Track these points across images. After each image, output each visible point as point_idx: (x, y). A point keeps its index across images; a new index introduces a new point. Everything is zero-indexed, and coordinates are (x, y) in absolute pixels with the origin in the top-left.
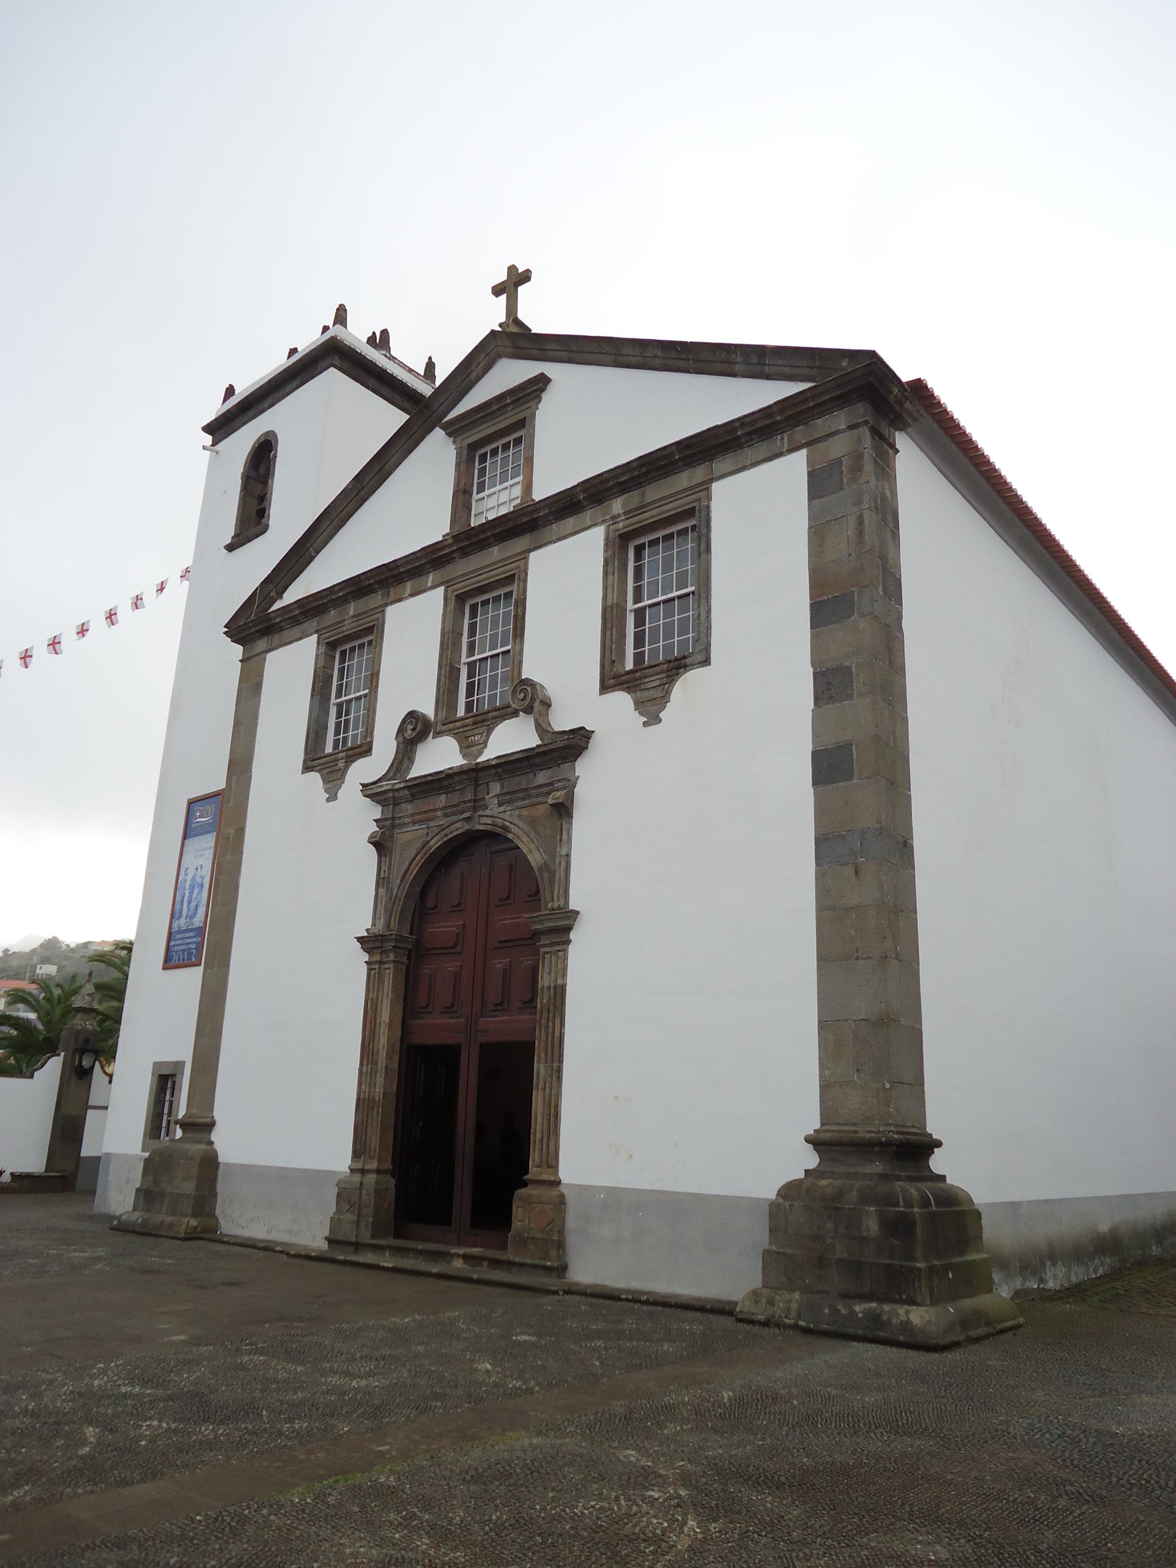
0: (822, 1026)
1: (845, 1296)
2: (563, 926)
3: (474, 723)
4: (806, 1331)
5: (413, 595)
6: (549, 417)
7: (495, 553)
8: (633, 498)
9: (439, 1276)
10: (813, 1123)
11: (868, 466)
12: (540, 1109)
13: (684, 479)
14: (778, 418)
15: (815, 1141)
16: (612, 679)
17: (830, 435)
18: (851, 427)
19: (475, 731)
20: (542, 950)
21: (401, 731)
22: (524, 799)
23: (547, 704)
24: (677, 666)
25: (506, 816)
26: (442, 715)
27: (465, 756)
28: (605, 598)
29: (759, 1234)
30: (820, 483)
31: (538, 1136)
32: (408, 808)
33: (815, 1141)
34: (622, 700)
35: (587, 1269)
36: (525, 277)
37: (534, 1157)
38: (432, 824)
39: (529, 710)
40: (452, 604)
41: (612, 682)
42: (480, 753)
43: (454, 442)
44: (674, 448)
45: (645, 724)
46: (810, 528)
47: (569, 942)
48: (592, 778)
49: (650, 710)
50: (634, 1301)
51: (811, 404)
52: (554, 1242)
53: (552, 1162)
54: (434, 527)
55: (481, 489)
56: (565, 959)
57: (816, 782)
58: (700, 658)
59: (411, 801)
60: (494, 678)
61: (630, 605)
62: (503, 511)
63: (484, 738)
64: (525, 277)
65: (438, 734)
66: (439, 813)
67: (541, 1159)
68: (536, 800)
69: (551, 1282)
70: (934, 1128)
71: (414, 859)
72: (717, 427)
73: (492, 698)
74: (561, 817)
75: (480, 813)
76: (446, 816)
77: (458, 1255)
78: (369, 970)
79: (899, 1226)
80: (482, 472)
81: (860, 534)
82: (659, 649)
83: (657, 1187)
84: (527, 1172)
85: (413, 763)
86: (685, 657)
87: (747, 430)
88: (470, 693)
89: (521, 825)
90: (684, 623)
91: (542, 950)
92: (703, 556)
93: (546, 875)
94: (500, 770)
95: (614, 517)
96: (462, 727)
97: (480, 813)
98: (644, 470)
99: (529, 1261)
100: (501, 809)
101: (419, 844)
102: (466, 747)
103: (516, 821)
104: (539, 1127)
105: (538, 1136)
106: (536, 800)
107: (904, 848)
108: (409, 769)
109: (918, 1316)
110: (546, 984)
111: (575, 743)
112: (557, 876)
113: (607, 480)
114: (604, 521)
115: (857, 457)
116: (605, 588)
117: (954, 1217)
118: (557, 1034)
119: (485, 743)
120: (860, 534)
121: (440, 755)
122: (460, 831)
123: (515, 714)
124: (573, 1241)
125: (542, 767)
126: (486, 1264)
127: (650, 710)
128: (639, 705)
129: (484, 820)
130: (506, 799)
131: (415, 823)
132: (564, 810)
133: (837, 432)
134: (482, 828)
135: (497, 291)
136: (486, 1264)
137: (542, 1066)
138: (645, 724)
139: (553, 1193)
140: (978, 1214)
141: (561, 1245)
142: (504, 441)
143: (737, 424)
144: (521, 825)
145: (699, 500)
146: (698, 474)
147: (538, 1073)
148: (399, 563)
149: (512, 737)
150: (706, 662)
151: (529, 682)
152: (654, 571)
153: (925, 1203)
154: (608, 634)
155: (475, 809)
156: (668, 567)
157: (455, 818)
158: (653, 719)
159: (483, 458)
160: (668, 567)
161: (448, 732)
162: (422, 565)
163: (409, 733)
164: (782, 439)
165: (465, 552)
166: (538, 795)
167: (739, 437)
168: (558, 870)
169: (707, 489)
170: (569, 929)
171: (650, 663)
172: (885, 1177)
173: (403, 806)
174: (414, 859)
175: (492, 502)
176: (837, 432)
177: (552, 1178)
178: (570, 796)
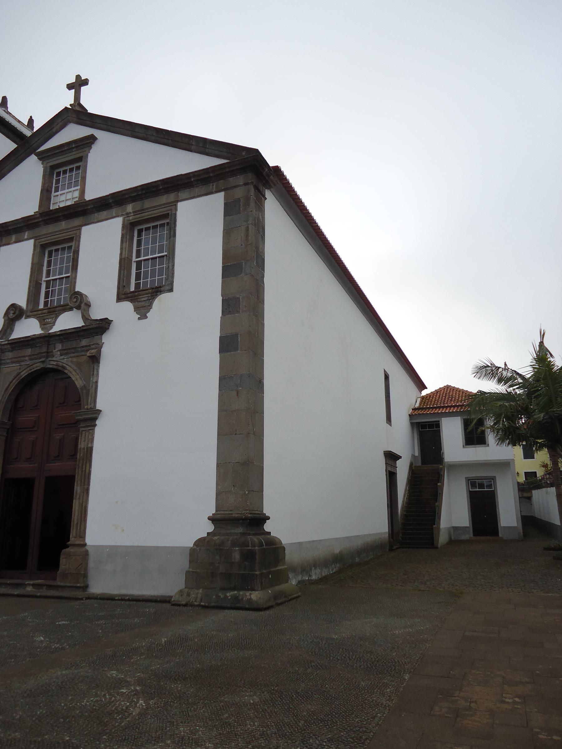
0: (218, 465)
1: (223, 589)
2: (93, 416)
3: (49, 312)
4: (204, 607)
5: (16, 242)
6: (95, 158)
7: (63, 225)
8: (138, 205)
9: (18, 596)
10: (212, 510)
11: (252, 204)
12: (77, 509)
13: (164, 199)
14: (211, 175)
15: (212, 519)
16: (123, 295)
17: (235, 187)
18: (245, 184)
19: (49, 317)
20: (81, 429)
21: (7, 314)
22: (74, 353)
23: (88, 305)
24: (156, 291)
25: (65, 361)
26: (30, 307)
27: (42, 329)
28: (121, 254)
29: (184, 563)
30: (230, 209)
31: (75, 522)
32: (10, 355)
33: (212, 519)
34: (128, 306)
35: (98, 586)
36: (85, 82)
37: (73, 533)
38: (23, 363)
39: (78, 308)
40: (38, 250)
41: (123, 296)
42: (51, 328)
43: (42, 164)
44: (159, 183)
45: (139, 319)
46: (224, 230)
47: (95, 425)
48: (110, 344)
49: (142, 311)
50: (122, 600)
51: (227, 170)
52: (82, 574)
53: (82, 535)
54: (29, 207)
55: (57, 190)
56: (93, 434)
57: (221, 351)
58: (168, 288)
59: (12, 351)
60: (60, 290)
61: (134, 259)
62: (69, 203)
63: (53, 320)
64: (85, 82)
65: (28, 317)
66: (27, 358)
67: (76, 534)
68: (81, 354)
69: (79, 594)
70: (267, 511)
71: (11, 382)
72: (181, 175)
73: (59, 300)
74: (93, 363)
75: (50, 359)
76: (31, 360)
77: (29, 585)
79: (248, 556)
80: (58, 182)
81: (247, 236)
82: (148, 282)
83: (136, 544)
84: (69, 541)
85: (12, 330)
86: (160, 287)
87: (196, 178)
88: (47, 296)
89: (72, 366)
90: (161, 270)
91: (81, 429)
92: (172, 238)
93: (85, 392)
94: (61, 337)
95: (127, 214)
96: (41, 314)
97: (50, 359)
98: (144, 192)
99: (69, 585)
100: (62, 357)
101: (15, 374)
102: (43, 325)
103: (70, 364)
104: (76, 518)
105: (75, 522)
106: (81, 354)
107: (260, 384)
108: (10, 334)
109: (255, 596)
110: (82, 446)
111: (104, 325)
112: (90, 392)
114: (122, 215)
115: (247, 199)
116: (121, 249)
117: (274, 550)
118: (87, 471)
119: (54, 324)
120: (247, 236)
121: (29, 328)
122: (38, 368)
123: (71, 309)
124: (92, 573)
125: (85, 337)
126: (45, 587)
127: (142, 311)
128: (136, 309)
130: (64, 352)
131: (13, 363)
132: (95, 359)
133: (239, 186)
134: (51, 366)
135: (70, 87)
136: (45, 587)
137: (79, 488)
138: (139, 319)
139: (82, 550)
140: (284, 548)
141: (85, 576)
142: (71, 166)
143: (191, 175)
144: (72, 366)
145: (171, 210)
146: (171, 197)
147: (77, 491)
149: (69, 321)
150: (171, 290)
151: (79, 293)
152: (147, 243)
153: (261, 545)
154: (122, 272)
155: (47, 357)
156: (154, 242)
157: (35, 361)
158: (143, 316)
159: (58, 174)
160: (154, 242)
161: (34, 316)
162: (22, 227)
163: (11, 315)
164: (213, 185)
165: (47, 222)
166: (82, 351)
167: (192, 182)
168: (91, 389)
169: (175, 205)
170: (96, 419)
171: (143, 288)
172: (243, 534)
173: (7, 354)
174: (11, 382)
175: (63, 198)
176: (239, 186)
177: (82, 543)
178: (99, 352)
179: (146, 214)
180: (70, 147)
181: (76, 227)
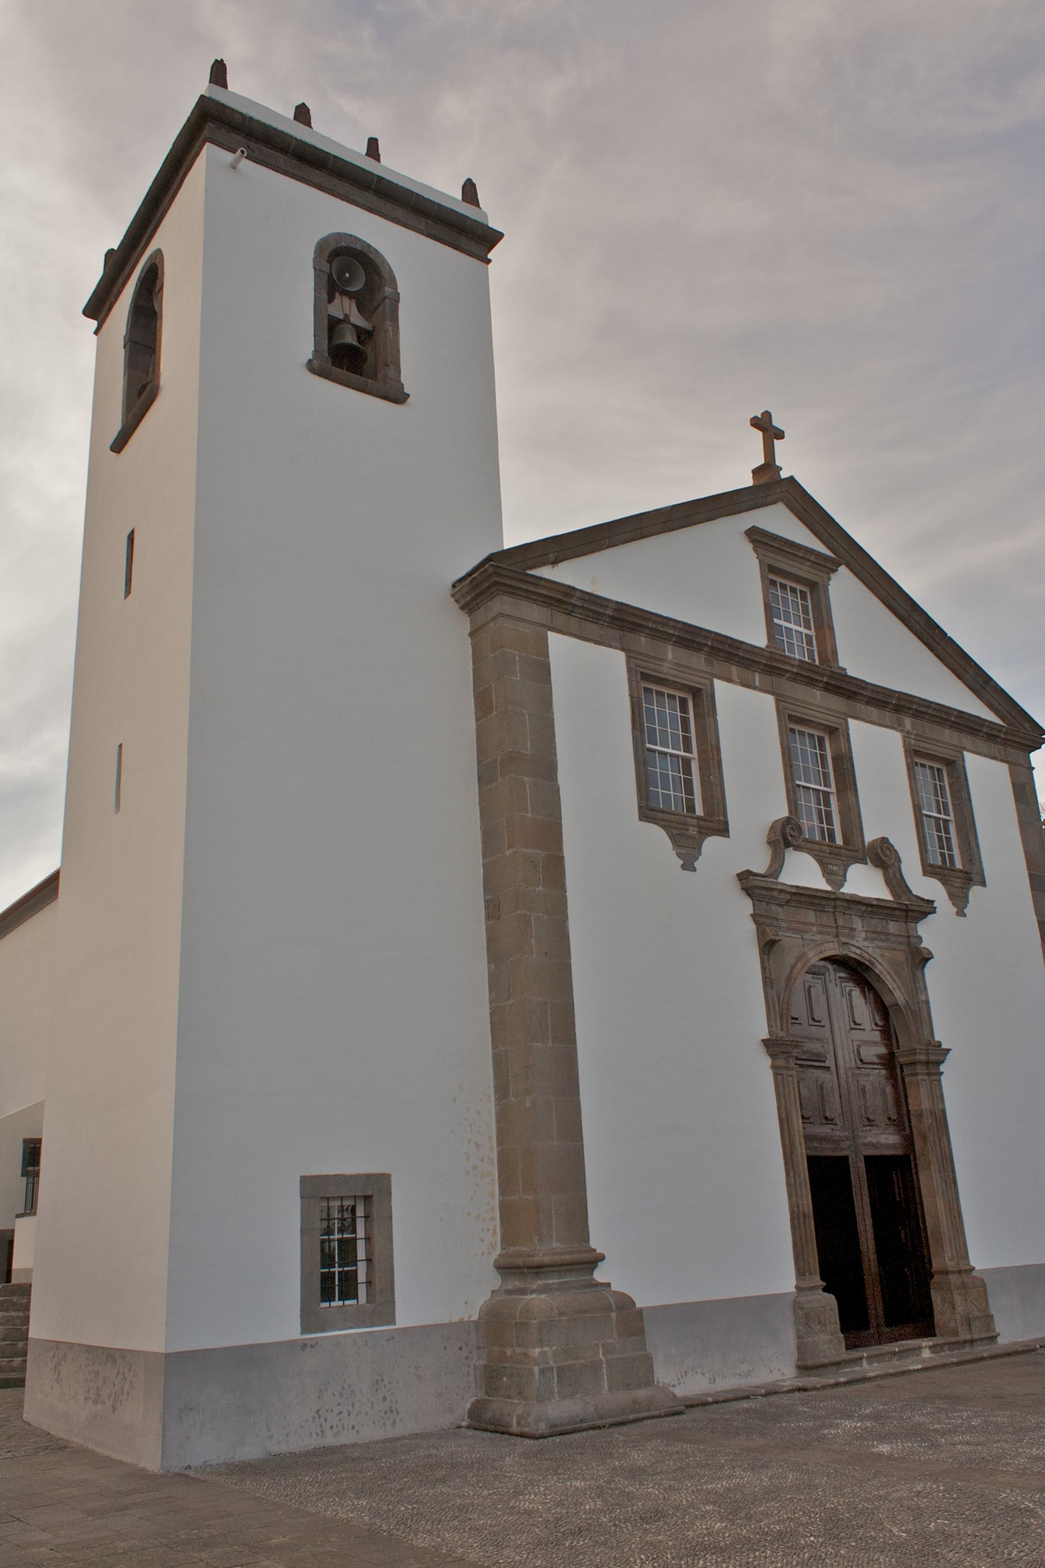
22: (882, 941)
27: (829, 881)
69: (983, 1350)
72: (980, 718)
76: (821, 933)
78: (776, 1075)
89: (884, 964)
95: (908, 732)
100: (866, 943)
111: (925, 909)
113: (913, 703)
114: (902, 731)
126: (946, 1348)
129: (854, 949)
134: (854, 956)
148: (743, 646)
161: (810, 851)
179: (928, 746)
180: (807, 556)
181: (840, 712)
